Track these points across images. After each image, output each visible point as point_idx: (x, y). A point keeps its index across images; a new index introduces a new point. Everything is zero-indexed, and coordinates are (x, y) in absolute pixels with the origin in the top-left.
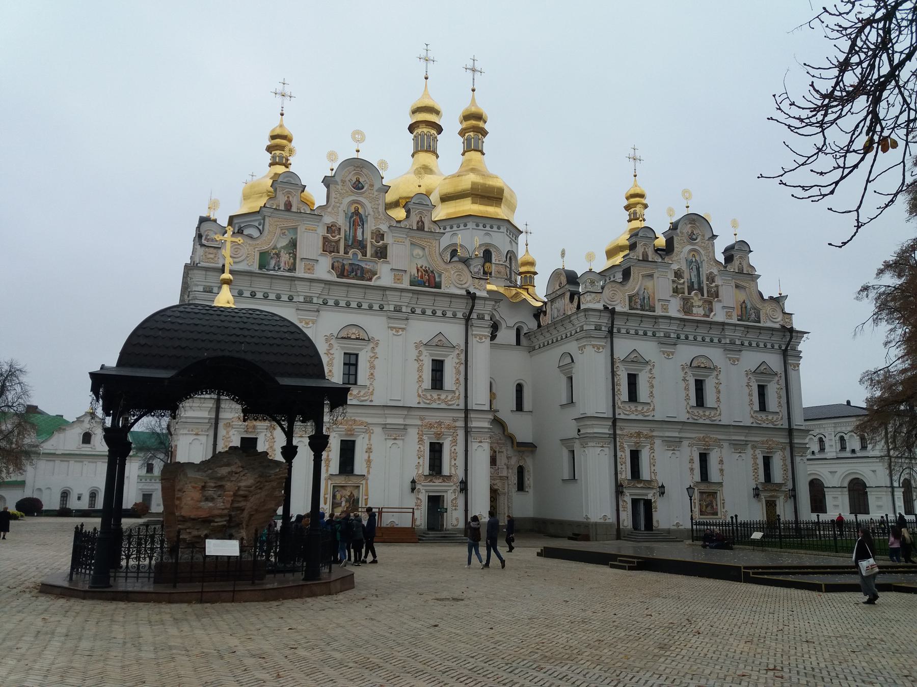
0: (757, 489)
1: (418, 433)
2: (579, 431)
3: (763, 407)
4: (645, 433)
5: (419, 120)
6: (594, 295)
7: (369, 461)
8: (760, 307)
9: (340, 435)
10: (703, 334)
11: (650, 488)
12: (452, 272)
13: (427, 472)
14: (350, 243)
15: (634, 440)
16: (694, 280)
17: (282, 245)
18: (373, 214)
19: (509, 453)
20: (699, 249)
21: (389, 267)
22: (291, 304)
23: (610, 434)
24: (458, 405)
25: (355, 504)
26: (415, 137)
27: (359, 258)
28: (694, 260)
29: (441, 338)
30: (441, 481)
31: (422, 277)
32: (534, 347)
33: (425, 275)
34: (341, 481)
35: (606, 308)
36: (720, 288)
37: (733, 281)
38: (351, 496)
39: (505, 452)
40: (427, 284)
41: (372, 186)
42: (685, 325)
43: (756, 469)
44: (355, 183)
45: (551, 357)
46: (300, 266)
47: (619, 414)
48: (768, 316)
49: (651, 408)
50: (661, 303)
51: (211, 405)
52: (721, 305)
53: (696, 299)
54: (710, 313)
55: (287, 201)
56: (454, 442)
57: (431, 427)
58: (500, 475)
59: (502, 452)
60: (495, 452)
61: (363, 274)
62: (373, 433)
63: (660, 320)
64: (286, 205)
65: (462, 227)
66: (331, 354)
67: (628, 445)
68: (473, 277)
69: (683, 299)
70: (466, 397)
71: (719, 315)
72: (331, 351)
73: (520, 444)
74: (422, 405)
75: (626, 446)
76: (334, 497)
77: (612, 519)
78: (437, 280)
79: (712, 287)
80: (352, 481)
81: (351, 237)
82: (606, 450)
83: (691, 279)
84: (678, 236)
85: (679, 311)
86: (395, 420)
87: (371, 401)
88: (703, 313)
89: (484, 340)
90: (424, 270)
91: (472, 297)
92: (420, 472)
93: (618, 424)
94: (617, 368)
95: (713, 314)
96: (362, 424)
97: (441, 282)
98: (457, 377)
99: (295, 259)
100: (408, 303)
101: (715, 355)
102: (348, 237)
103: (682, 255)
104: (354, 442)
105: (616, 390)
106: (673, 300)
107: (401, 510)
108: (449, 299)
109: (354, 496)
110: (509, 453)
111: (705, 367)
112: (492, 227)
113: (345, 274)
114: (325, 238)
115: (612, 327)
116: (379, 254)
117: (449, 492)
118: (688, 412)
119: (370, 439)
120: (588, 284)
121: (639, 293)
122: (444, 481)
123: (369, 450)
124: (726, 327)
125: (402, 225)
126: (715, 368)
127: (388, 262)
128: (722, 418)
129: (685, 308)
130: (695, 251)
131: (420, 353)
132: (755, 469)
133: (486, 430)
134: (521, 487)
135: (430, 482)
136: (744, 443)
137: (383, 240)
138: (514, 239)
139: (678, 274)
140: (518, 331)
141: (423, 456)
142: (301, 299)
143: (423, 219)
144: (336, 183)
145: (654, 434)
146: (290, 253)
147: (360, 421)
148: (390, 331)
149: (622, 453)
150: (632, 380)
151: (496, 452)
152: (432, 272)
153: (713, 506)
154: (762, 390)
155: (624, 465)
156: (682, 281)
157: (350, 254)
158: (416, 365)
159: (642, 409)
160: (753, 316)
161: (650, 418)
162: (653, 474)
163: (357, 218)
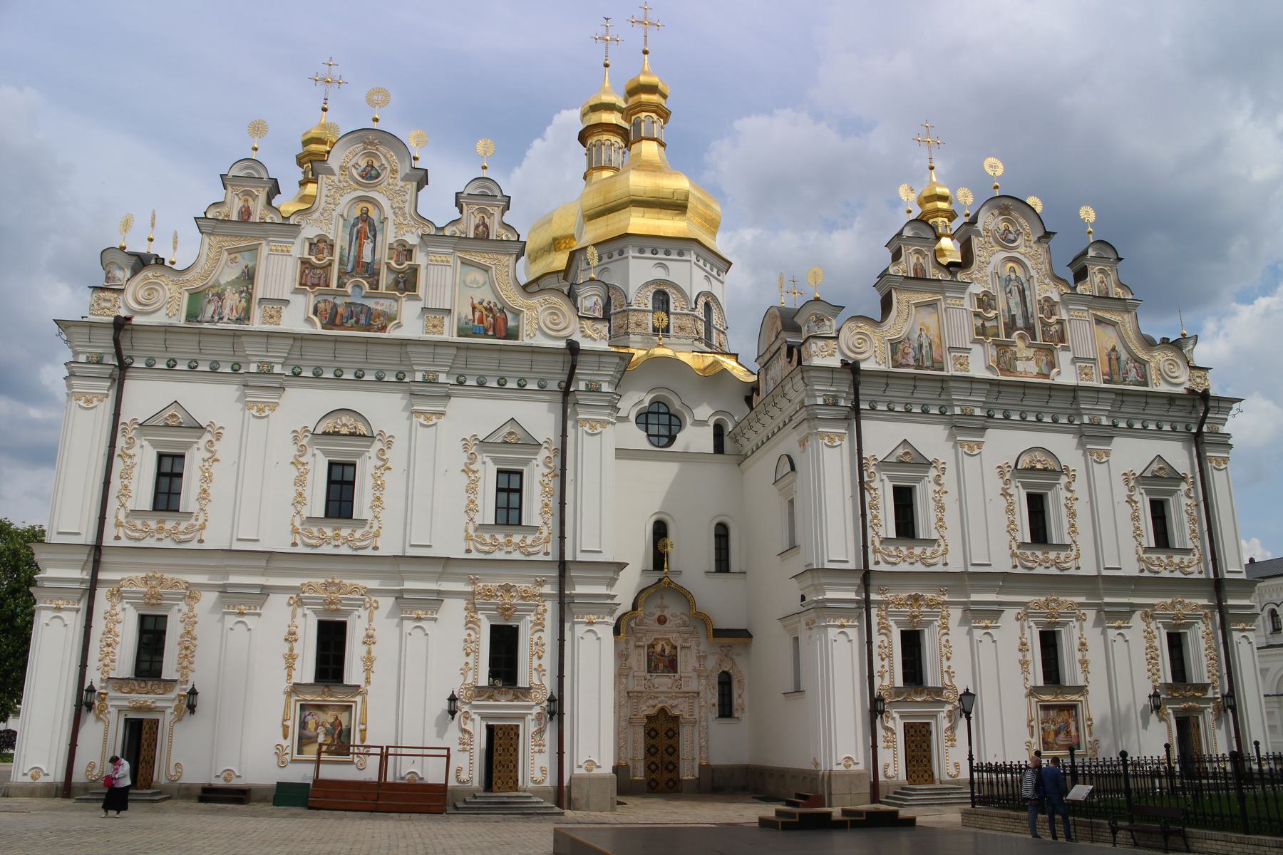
0: (1156, 695)
1: (466, 609)
2: (803, 598)
3: (1163, 539)
5: (591, 123)
6: (821, 343)
7: (369, 661)
8: (1145, 357)
9: (315, 611)
10: (1038, 409)
11: (940, 701)
12: (540, 309)
13: (484, 680)
14: (349, 268)
16: (1017, 311)
17: (229, 280)
18: (394, 217)
19: (702, 647)
20: (1022, 257)
21: (420, 305)
22: (238, 379)
23: (857, 602)
24: (547, 554)
25: (342, 738)
26: (588, 150)
27: (364, 292)
28: (1013, 276)
30: (510, 697)
31: (481, 321)
32: (746, 455)
33: (487, 316)
35: (845, 364)
36: (1067, 326)
37: (1090, 311)
38: (337, 723)
40: (491, 333)
41: (394, 171)
42: (999, 392)
43: (1152, 659)
44: (364, 170)
45: (763, 466)
46: (257, 313)
47: (877, 563)
48: (1161, 375)
49: (942, 548)
50: (953, 354)
51: (85, 557)
52: (1069, 355)
53: (1021, 348)
54: (1050, 372)
55: (244, 206)
56: (539, 625)
57: (492, 596)
58: (684, 689)
59: (688, 648)
60: (675, 648)
61: (370, 320)
62: (377, 608)
63: (951, 384)
64: (241, 213)
65: (616, 256)
66: (303, 464)
67: (897, 623)
68: (580, 317)
69: (997, 346)
70: (562, 537)
71: (1066, 375)
72: (301, 459)
73: (718, 633)
74: (475, 555)
75: (892, 623)
76: (303, 725)
77: (861, 764)
78: (511, 323)
79: (1050, 325)
81: (352, 258)
82: (853, 633)
83: (1009, 310)
84: (981, 237)
85: (989, 368)
87: (376, 548)
88: (1035, 370)
90: (486, 309)
91: (573, 348)
92: (470, 680)
94: (869, 477)
95: (1055, 370)
96: (355, 589)
97: (518, 327)
98: (546, 500)
99: (249, 301)
100: (451, 367)
101: (1063, 446)
102: (345, 259)
103: (990, 269)
104: (344, 624)
105: (869, 517)
106: (977, 349)
107: (422, 752)
108: (528, 357)
109: (341, 724)
110: (702, 647)
111: (1045, 469)
112: (667, 253)
113: (338, 321)
114: (305, 262)
115: (857, 401)
116: (401, 285)
118: (1014, 555)
119: (370, 620)
120: (812, 324)
122: (516, 698)
123: (369, 639)
124: (1080, 394)
125: (447, 232)
126: (1062, 471)
127: (417, 298)
128: (1081, 562)
129: (1002, 359)
130: (1014, 262)
132: (1152, 658)
134: (726, 709)
135: (490, 697)
136: (1127, 609)
137: (411, 260)
138: (714, 273)
139: (985, 301)
140: (719, 431)
141: (476, 651)
142: (253, 368)
143: (487, 220)
144: (330, 172)
146: (242, 292)
147: (351, 585)
148: (414, 419)
149: (883, 637)
150: (904, 500)
151: (675, 648)
152: (501, 311)
153: (1068, 733)
154: (1159, 511)
155: (887, 660)
156: (992, 314)
157: (349, 289)
158: (465, 480)
159: (924, 553)
160: (1133, 374)
162: (946, 675)
163: (365, 227)
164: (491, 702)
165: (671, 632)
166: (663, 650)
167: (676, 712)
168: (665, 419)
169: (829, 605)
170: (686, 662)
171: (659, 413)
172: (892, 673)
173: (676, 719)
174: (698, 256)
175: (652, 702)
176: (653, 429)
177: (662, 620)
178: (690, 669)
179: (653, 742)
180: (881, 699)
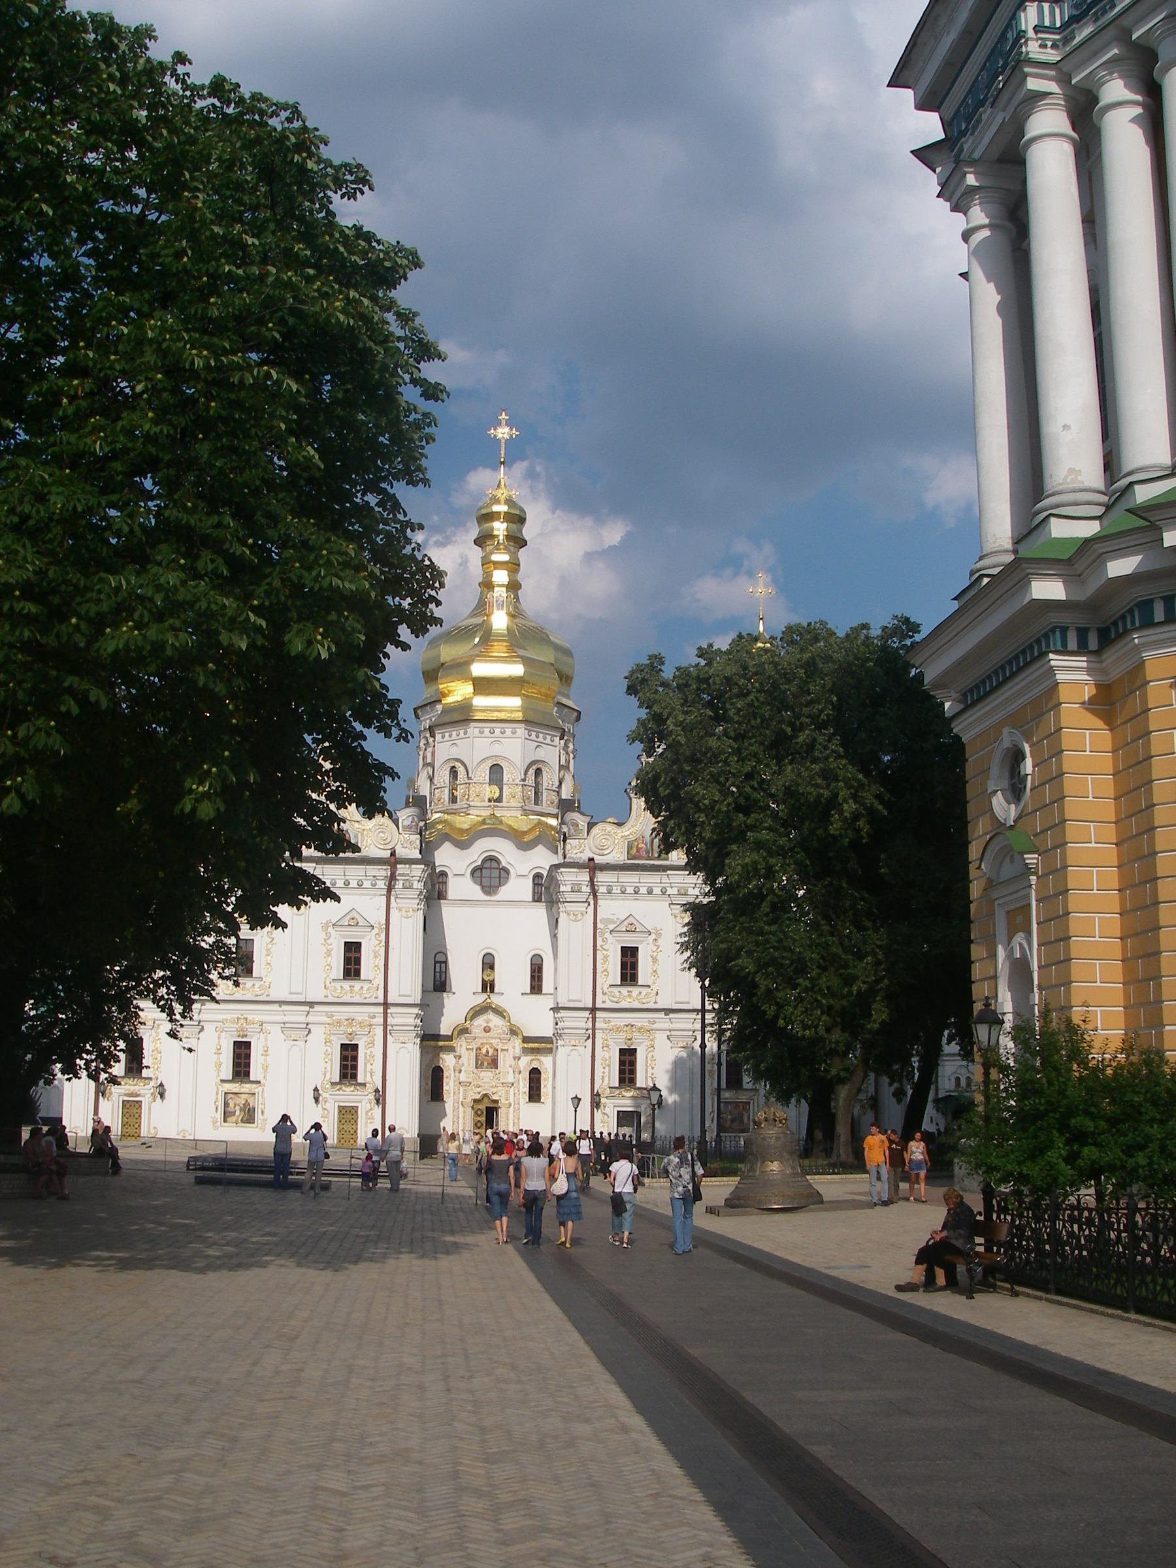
2: (557, 1024)
4: (640, 1025)
7: (265, 1068)
9: (232, 1036)
15: (623, 1035)
19: (518, 1051)
24: (376, 998)
29: (354, 914)
30: (352, 1089)
34: (234, 1087)
38: (247, 1104)
39: (511, 1051)
47: (604, 1002)
58: (502, 1081)
73: (526, 1040)
76: (226, 1104)
80: (246, 1087)
86: (297, 1015)
89: (411, 913)
91: (393, 861)
92: (328, 1078)
93: (599, 1014)
104: (250, 1043)
117: (363, 1102)
119: (266, 1040)
121: (644, 835)
123: (266, 1052)
131: (329, 936)
133: (412, 1028)
134: (535, 1094)
138: (548, 740)
141: (331, 1060)
145: (654, 1026)
150: (629, 955)
153: (742, 1122)
161: (651, 1006)
162: (649, 1079)
164: (341, 1092)
165: (496, 1038)
166: (488, 1052)
167: (495, 1097)
168: (496, 873)
169: (566, 1031)
170: (505, 1061)
171: (491, 868)
172: (609, 1074)
173: (497, 1101)
174: (530, 731)
175: (479, 1090)
176: (486, 882)
177: (487, 1030)
178: (508, 1066)
179: (479, 1119)
180: (598, 1095)
